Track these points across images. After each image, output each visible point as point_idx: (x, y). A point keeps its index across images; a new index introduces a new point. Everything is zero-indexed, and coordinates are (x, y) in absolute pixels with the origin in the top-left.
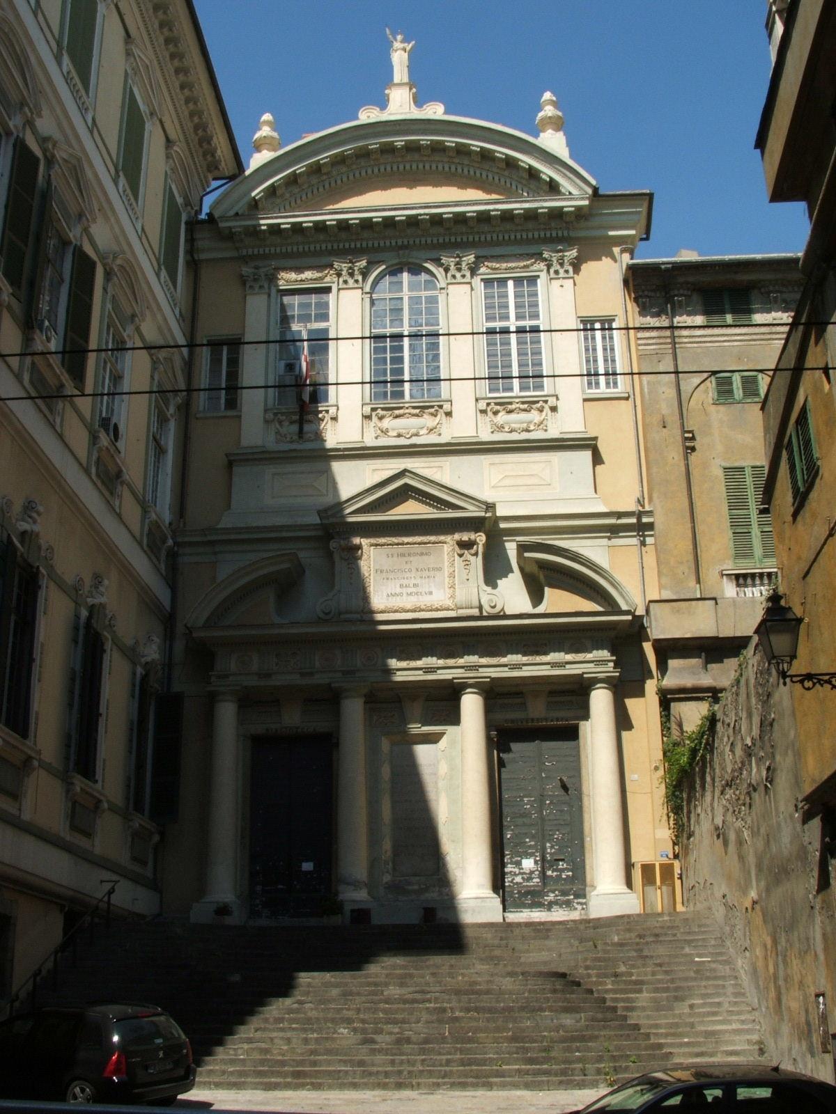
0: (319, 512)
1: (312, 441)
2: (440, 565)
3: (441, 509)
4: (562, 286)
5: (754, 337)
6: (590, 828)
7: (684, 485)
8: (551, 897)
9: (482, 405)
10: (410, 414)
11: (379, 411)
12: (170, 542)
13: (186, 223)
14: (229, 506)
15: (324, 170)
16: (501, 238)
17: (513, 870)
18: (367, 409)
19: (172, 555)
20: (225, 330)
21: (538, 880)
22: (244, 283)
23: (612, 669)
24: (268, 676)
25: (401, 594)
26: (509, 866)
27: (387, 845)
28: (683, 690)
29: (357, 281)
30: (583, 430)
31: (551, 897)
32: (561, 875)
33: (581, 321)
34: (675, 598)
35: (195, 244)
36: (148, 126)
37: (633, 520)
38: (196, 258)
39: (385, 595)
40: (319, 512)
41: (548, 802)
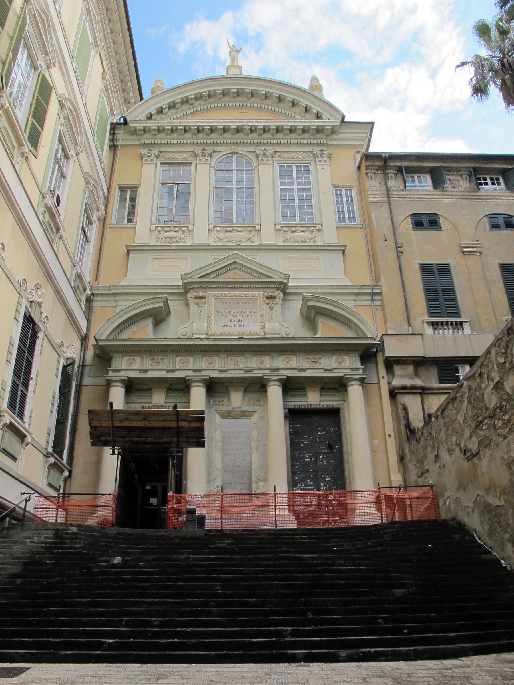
3: (256, 276)
5: (434, 196)
6: (349, 473)
9: (279, 227)
11: (218, 228)
12: (88, 292)
14: (126, 276)
18: (211, 227)
19: (89, 300)
22: (142, 158)
24: (146, 371)
28: (404, 388)
37: (370, 291)
38: (115, 143)
41: (321, 457)
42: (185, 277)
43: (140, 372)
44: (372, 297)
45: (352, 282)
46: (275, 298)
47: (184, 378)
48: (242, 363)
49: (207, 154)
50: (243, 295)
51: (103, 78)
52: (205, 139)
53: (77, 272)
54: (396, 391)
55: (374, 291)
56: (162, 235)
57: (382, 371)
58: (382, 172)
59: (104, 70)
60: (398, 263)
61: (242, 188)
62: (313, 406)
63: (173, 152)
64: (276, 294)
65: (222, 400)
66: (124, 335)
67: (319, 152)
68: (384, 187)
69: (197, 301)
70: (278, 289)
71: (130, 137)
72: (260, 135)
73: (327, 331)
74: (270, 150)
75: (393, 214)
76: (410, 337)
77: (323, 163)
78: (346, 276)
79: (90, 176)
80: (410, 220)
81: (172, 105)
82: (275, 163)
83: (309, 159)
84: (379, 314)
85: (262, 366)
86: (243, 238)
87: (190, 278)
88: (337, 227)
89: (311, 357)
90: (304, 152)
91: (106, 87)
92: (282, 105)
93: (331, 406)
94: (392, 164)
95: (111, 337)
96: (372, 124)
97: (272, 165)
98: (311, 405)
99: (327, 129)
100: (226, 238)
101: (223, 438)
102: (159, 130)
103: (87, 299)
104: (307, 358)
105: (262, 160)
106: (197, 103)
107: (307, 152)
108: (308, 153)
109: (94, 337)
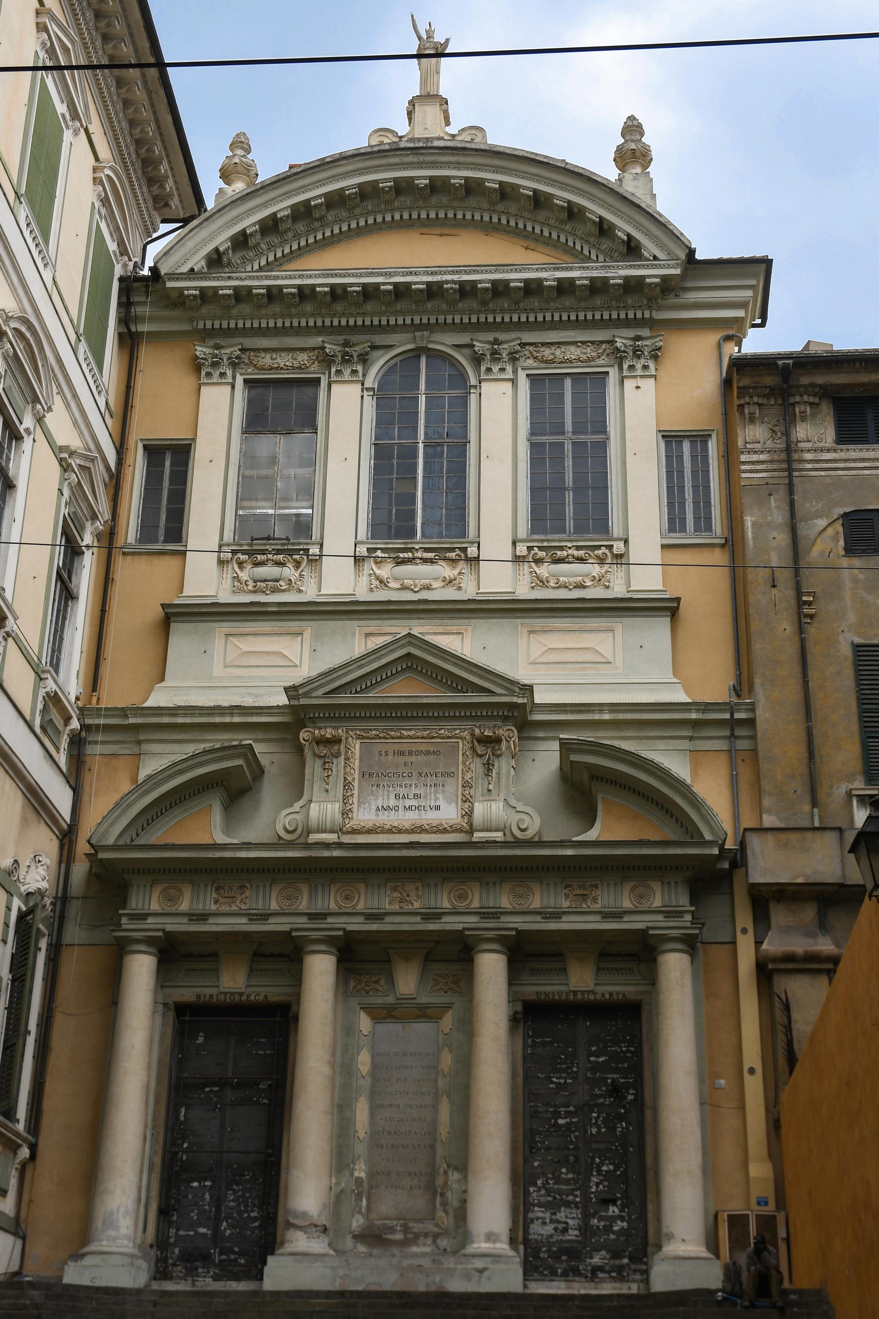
0: (287, 689)
1: (283, 591)
2: (452, 770)
4: (638, 387)
7: (798, 669)
8: (596, 1260)
10: (421, 559)
11: (379, 553)
13: (121, 279)
14: (162, 679)
15: (317, 214)
16: (557, 318)
17: (541, 1215)
18: (362, 550)
19: (77, 743)
20: (170, 431)
21: (577, 1232)
23: (689, 924)
25: (396, 808)
26: (536, 1209)
27: (361, 1172)
28: (790, 958)
29: (354, 372)
30: (662, 588)
31: (596, 1260)
32: (612, 1226)
33: (663, 436)
34: (782, 826)
35: (133, 310)
36: (68, 135)
38: (133, 329)
39: (374, 808)
40: (287, 689)
42: (293, 693)
43: (190, 920)
44: (732, 730)
45: (688, 693)
46: (498, 740)
47: (289, 933)
48: (418, 897)
49: (355, 355)
50: (426, 733)
51: (96, 181)
52: (351, 315)
53: (47, 693)
54: (770, 966)
55: (737, 716)
56: (246, 571)
57: (744, 919)
58: (780, 402)
59: (97, 159)
60: (797, 645)
61: (441, 445)
62: (579, 996)
63: (274, 350)
64: (501, 732)
65: (374, 979)
66: (155, 836)
67: (629, 343)
68: (780, 445)
69: (324, 751)
70: (505, 719)
71: (167, 313)
72: (484, 303)
73: (611, 828)
74: (510, 340)
75: (799, 513)
76: (809, 835)
77: (639, 372)
78: (675, 675)
79: (72, 454)
80: (841, 529)
81: (271, 223)
82: (522, 375)
83: (602, 364)
84: (745, 772)
85: (461, 905)
86: (436, 579)
87: (306, 695)
88: (664, 547)
89: (575, 885)
90: (593, 343)
91: (105, 201)
92: (542, 215)
93: (620, 997)
94: (805, 380)
95: (126, 840)
96: (767, 263)
97: (514, 381)
98: (575, 993)
99: (650, 284)
100: (396, 579)
101: (375, 1066)
102: (241, 295)
103: (71, 739)
104: (566, 887)
105: (489, 370)
106: (330, 217)
107: (602, 342)
108: (604, 346)
109: (89, 842)
